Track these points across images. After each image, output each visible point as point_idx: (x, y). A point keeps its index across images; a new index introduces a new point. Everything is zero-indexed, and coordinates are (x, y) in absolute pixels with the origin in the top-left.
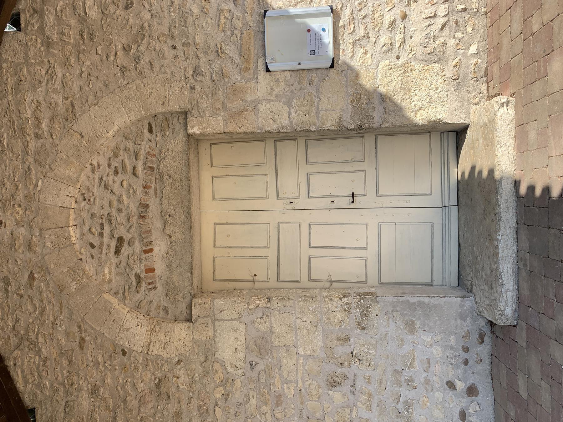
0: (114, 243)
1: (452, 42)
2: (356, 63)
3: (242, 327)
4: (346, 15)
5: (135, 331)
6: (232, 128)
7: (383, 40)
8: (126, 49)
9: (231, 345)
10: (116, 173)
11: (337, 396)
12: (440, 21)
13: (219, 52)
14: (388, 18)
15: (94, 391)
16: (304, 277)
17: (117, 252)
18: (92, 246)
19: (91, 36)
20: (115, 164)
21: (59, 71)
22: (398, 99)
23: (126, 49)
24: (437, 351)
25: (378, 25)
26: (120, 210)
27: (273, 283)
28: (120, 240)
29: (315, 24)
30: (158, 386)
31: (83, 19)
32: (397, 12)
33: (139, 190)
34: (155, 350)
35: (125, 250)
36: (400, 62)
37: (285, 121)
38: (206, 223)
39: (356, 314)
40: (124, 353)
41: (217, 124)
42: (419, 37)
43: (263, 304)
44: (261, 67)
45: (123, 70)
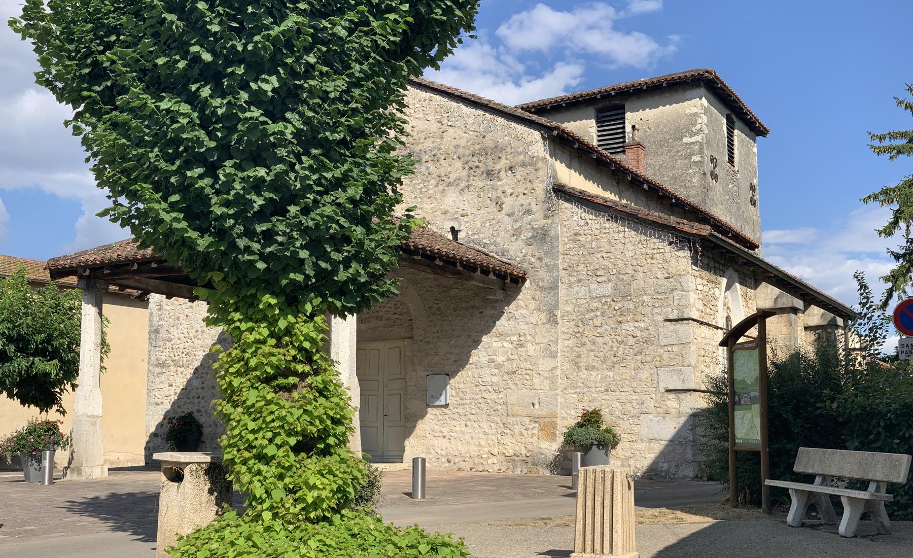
1: (431, 456)
2: (428, 416)
4: (446, 411)
7: (436, 427)
12: (439, 452)
13: (436, 353)
14: (443, 429)
19: (444, 292)
20: (399, 304)
22: (414, 434)
25: (442, 425)
29: (443, 398)
31: (451, 288)
32: (446, 433)
33: (388, 316)
36: (428, 435)
42: (435, 442)
45: (431, 307)
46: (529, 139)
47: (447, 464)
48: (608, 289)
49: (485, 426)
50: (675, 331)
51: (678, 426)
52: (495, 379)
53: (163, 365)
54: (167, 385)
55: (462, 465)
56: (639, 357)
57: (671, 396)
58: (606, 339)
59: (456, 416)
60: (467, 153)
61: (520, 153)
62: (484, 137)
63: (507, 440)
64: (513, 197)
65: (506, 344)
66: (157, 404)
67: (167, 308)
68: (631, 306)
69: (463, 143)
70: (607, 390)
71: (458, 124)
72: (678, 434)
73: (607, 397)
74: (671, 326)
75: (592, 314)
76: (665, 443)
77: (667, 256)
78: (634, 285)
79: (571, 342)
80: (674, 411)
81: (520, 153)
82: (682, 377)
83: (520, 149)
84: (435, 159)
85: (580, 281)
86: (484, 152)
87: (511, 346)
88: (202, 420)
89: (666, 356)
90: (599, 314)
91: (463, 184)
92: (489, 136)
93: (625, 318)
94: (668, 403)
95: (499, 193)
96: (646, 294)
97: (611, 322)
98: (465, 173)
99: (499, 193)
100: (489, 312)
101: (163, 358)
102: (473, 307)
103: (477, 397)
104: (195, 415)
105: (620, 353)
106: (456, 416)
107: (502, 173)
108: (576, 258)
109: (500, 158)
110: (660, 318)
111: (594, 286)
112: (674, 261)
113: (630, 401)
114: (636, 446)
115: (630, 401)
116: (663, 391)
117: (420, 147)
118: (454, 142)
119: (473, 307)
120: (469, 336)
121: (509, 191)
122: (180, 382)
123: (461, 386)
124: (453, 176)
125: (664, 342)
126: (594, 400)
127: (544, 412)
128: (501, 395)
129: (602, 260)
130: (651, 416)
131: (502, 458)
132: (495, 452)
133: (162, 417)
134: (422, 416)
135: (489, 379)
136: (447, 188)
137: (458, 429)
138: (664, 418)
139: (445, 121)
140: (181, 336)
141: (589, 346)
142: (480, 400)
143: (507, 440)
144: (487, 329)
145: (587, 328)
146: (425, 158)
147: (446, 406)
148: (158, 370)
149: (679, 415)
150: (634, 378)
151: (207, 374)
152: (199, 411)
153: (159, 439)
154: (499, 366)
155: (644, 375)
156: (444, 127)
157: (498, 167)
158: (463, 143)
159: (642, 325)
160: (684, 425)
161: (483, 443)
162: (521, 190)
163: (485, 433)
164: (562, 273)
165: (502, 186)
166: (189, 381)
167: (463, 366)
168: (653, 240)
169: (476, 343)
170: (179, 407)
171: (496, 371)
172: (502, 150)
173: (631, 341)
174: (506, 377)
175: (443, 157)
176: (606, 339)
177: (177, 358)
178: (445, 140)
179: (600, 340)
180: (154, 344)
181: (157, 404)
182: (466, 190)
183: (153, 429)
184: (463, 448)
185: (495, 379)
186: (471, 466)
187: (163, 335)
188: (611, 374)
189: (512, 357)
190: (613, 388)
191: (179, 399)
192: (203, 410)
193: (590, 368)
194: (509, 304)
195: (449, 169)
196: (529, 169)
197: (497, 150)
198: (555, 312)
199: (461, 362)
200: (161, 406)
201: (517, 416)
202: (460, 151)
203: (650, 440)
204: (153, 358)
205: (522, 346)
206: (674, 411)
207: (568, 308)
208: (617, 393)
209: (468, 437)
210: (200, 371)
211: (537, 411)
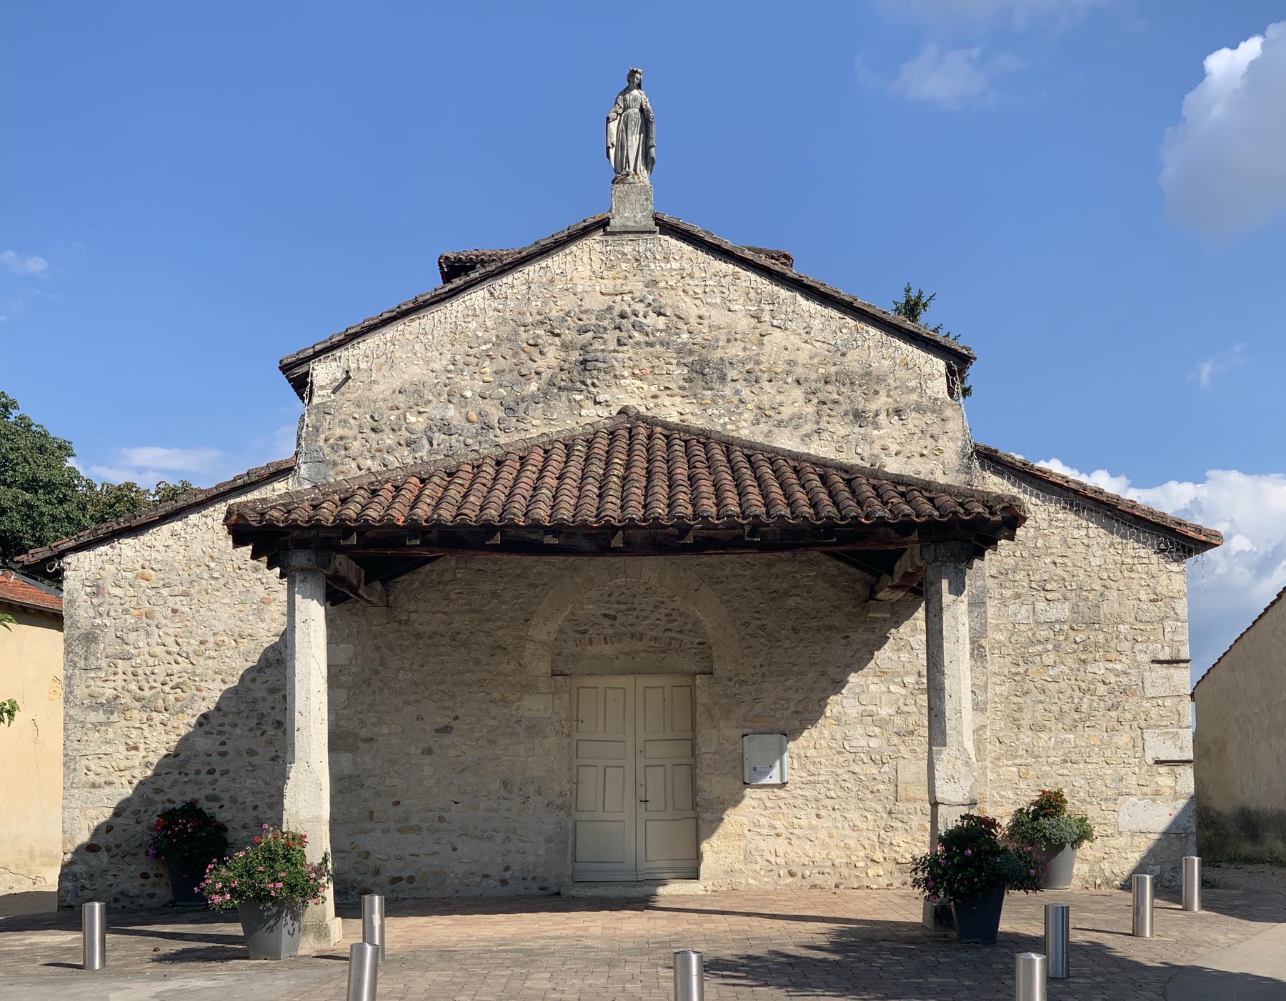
0: (612, 613)
1: (757, 867)
2: (747, 801)
3: (548, 715)
5: (544, 630)
6: (700, 709)
7: (762, 820)
8: (762, 627)
9: (535, 706)
10: (667, 615)
11: (496, 786)
12: (773, 859)
14: (778, 824)
15: (495, 595)
16: (580, 762)
17: (605, 615)
18: (610, 596)
19: (773, 600)
20: (674, 614)
21: (748, 573)
22: (720, 831)
23: (762, 627)
24: (532, 859)
26: (638, 617)
27: (577, 736)
28: (615, 618)
29: (776, 772)
30: (500, 647)
31: (787, 594)
32: (781, 830)
33: (654, 633)
34: (529, 645)
35: (606, 622)
36: (746, 832)
37: (703, 750)
38: (626, 681)
39: (559, 801)
40: (527, 620)
41: (703, 699)
42: (763, 845)
43: (566, 731)
44: (746, 731)
46: (927, 369)
47: (790, 880)
48: (1062, 611)
49: (854, 816)
50: (1168, 678)
51: (1175, 813)
52: (874, 743)
53: (110, 706)
54: (122, 748)
55: (819, 880)
56: (1114, 714)
57: (1163, 770)
58: (1062, 684)
59: (799, 802)
60: (813, 376)
61: (913, 390)
62: (843, 355)
63: (899, 838)
64: (901, 459)
65: (893, 688)
66: (94, 786)
67: (117, 591)
68: (1101, 638)
69: (802, 357)
70: (1065, 761)
71: (793, 325)
72: (1175, 823)
73: (1065, 772)
74: (1161, 670)
75: (1040, 648)
76: (1156, 836)
77: (1154, 568)
78: (1105, 608)
79: (1004, 689)
80: (1167, 791)
81: (913, 390)
82: (1179, 743)
83: (912, 384)
84: (752, 378)
85: (1018, 596)
86: (844, 378)
87: (903, 691)
88: (221, 816)
89: (1154, 713)
90: (1050, 647)
91: (809, 427)
92: (853, 355)
93: (1091, 656)
94: (1159, 779)
95: (877, 449)
96: (1123, 622)
97: (1070, 661)
98: (810, 409)
99: (877, 449)
100: (860, 635)
101: (109, 693)
102: (830, 628)
103: (839, 771)
104: (204, 805)
105: (1085, 707)
106: (799, 802)
107: (882, 417)
108: (1011, 561)
109: (877, 393)
110: (1145, 658)
111: (1041, 605)
112: (1164, 577)
113: (1101, 778)
114: (1113, 842)
115: (1101, 778)
116: (1151, 762)
117: (719, 354)
118: (786, 356)
119: (830, 628)
120: (823, 674)
121: (894, 448)
122: (160, 740)
123: (811, 753)
124: (787, 412)
125: (1150, 692)
126: (1045, 775)
128: (885, 768)
129: (1053, 567)
130: (1133, 799)
131: (891, 866)
132: (878, 856)
133: (109, 813)
134: (736, 802)
135: (863, 743)
136: (776, 430)
137: (804, 822)
138: (1154, 801)
139: (767, 317)
140: (159, 650)
141: (1035, 694)
142: (846, 776)
143: (899, 838)
144: (859, 663)
145: (1033, 669)
146: (732, 374)
147: (783, 785)
148: (100, 716)
149: (1176, 796)
150: (1108, 744)
151: (235, 725)
152: (208, 798)
153: (104, 857)
154: (883, 724)
155: (1123, 739)
156: (764, 327)
157: (873, 406)
158: (802, 357)
159: (1119, 667)
160: (1184, 810)
161: (852, 843)
162: (916, 447)
163: (854, 828)
164: (991, 583)
165: (880, 437)
166: (185, 740)
167: (813, 722)
168: (1131, 543)
169: (838, 685)
170: (158, 791)
171: (877, 730)
172: (880, 380)
173: (1102, 689)
174: (896, 740)
175: (766, 376)
176: (1062, 684)
177: (147, 693)
178: (767, 349)
179: (1053, 687)
180: (82, 663)
181: (94, 786)
182: (815, 437)
183: (84, 837)
184: (819, 856)
185: (874, 743)
186: (836, 880)
187: (107, 643)
188: (1071, 736)
189: (906, 709)
190: (1074, 757)
191: (156, 774)
193: (1037, 728)
194: (897, 624)
195: (779, 398)
196: (929, 417)
197: (870, 380)
198: (983, 642)
199: (807, 713)
200: (107, 790)
201: (916, 800)
202: (800, 371)
203: (1133, 834)
204: (80, 692)
206: (1167, 791)
207: (1000, 637)
208: (1082, 766)
209: (823, 835)
210: (215, 722)
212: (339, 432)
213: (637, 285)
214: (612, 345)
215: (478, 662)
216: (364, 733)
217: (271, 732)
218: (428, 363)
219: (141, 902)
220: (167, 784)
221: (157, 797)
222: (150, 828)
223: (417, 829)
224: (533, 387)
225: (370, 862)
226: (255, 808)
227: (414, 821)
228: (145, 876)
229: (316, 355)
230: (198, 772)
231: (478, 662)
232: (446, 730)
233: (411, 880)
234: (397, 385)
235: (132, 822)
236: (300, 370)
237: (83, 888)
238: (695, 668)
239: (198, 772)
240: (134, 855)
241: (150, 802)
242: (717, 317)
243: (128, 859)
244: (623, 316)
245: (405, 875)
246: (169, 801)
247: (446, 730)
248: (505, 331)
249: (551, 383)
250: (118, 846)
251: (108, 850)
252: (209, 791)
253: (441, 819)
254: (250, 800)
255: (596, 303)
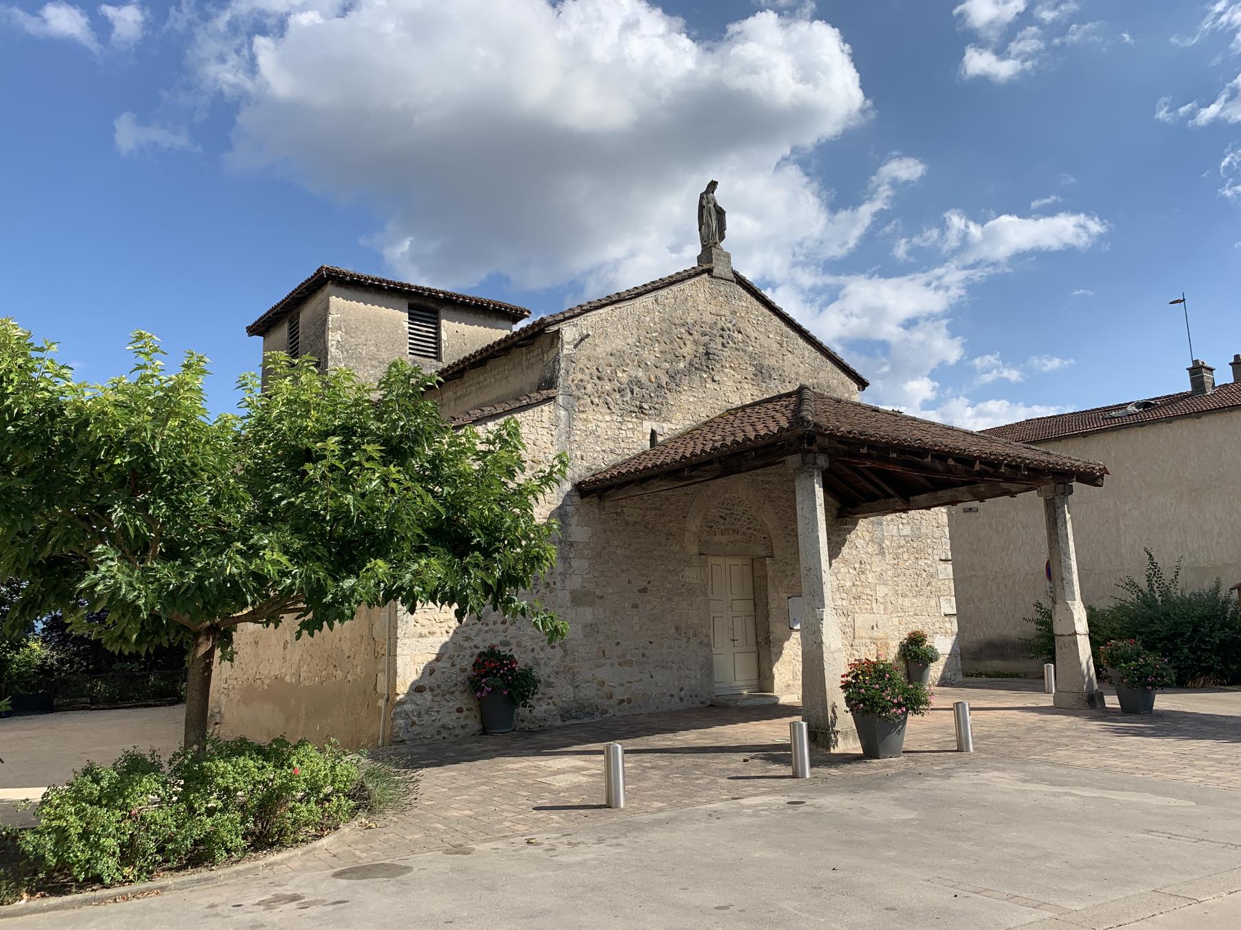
5: (694, 525)
11: (673, 630)
34: (687, 534)
35: (721, 521)
66: (421, 636)
92: (822, 374)
110: (937, 558)
127: (881, 635)
133: (434, 657)
170: (467, 639)
173: (924, 575)
181: (421, 636)
192: (513, 641)
200: (431, 639)
205: (863, 573)
211: (876, 634)
212: (580, 376)
213: (726, 311)
214: (720, 347)
215: (660, 545)
216: (598, 592)
217: (543, 591)
218: (625, 338)
219: (457, 732)
220: (474, 633)
221: (467, 644)
222: (463, 670)
223: (630, 663)
224: (682, 365)
225: (605, 689)
226: (533, 650)
227: (629, 657)
228: (460, 710)
229: (566, 319)
230: (495, 623)
231: (660, 545)
232: (644, 590)
233: (629, 701)
234: (609, 350)
235: (449, 665)
236: (555, 328)
237: (414, 723)
238: (763, 554)
239: (495, 623)
240: (452, 693)
241: (462, 648)
242: (765, 341)
243: (447, 697)
244: (723, 330)
245: (625, 698)
246: (476, 647)
247: (644, 590)
248: (665, 326)
249: (691, 364)
250: (438, 686)
251: (432, 690)
252: (502, 638)
253: (643, 655)
254: (529, 644)
255: (709, 319)
